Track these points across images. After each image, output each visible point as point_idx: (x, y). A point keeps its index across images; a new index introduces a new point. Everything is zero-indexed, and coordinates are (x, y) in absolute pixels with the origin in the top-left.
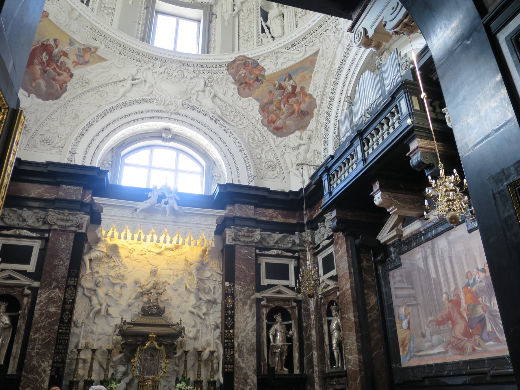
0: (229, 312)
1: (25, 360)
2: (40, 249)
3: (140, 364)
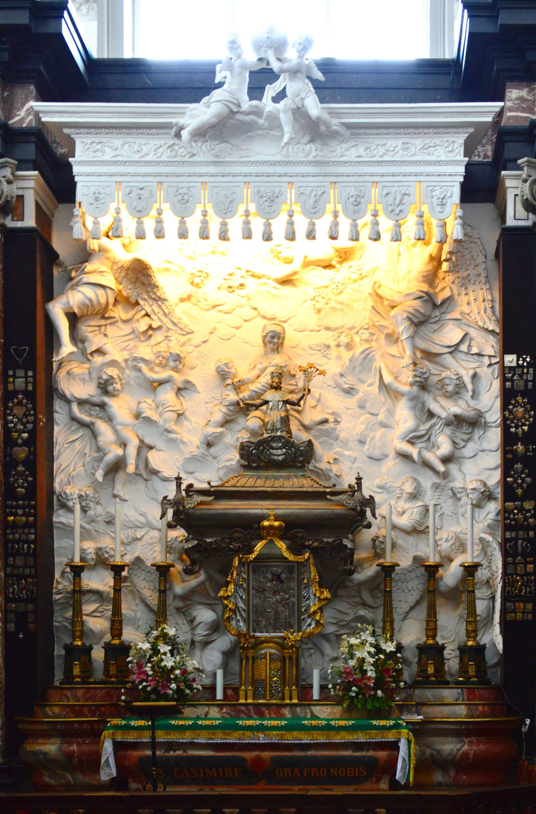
3: (247, 602)
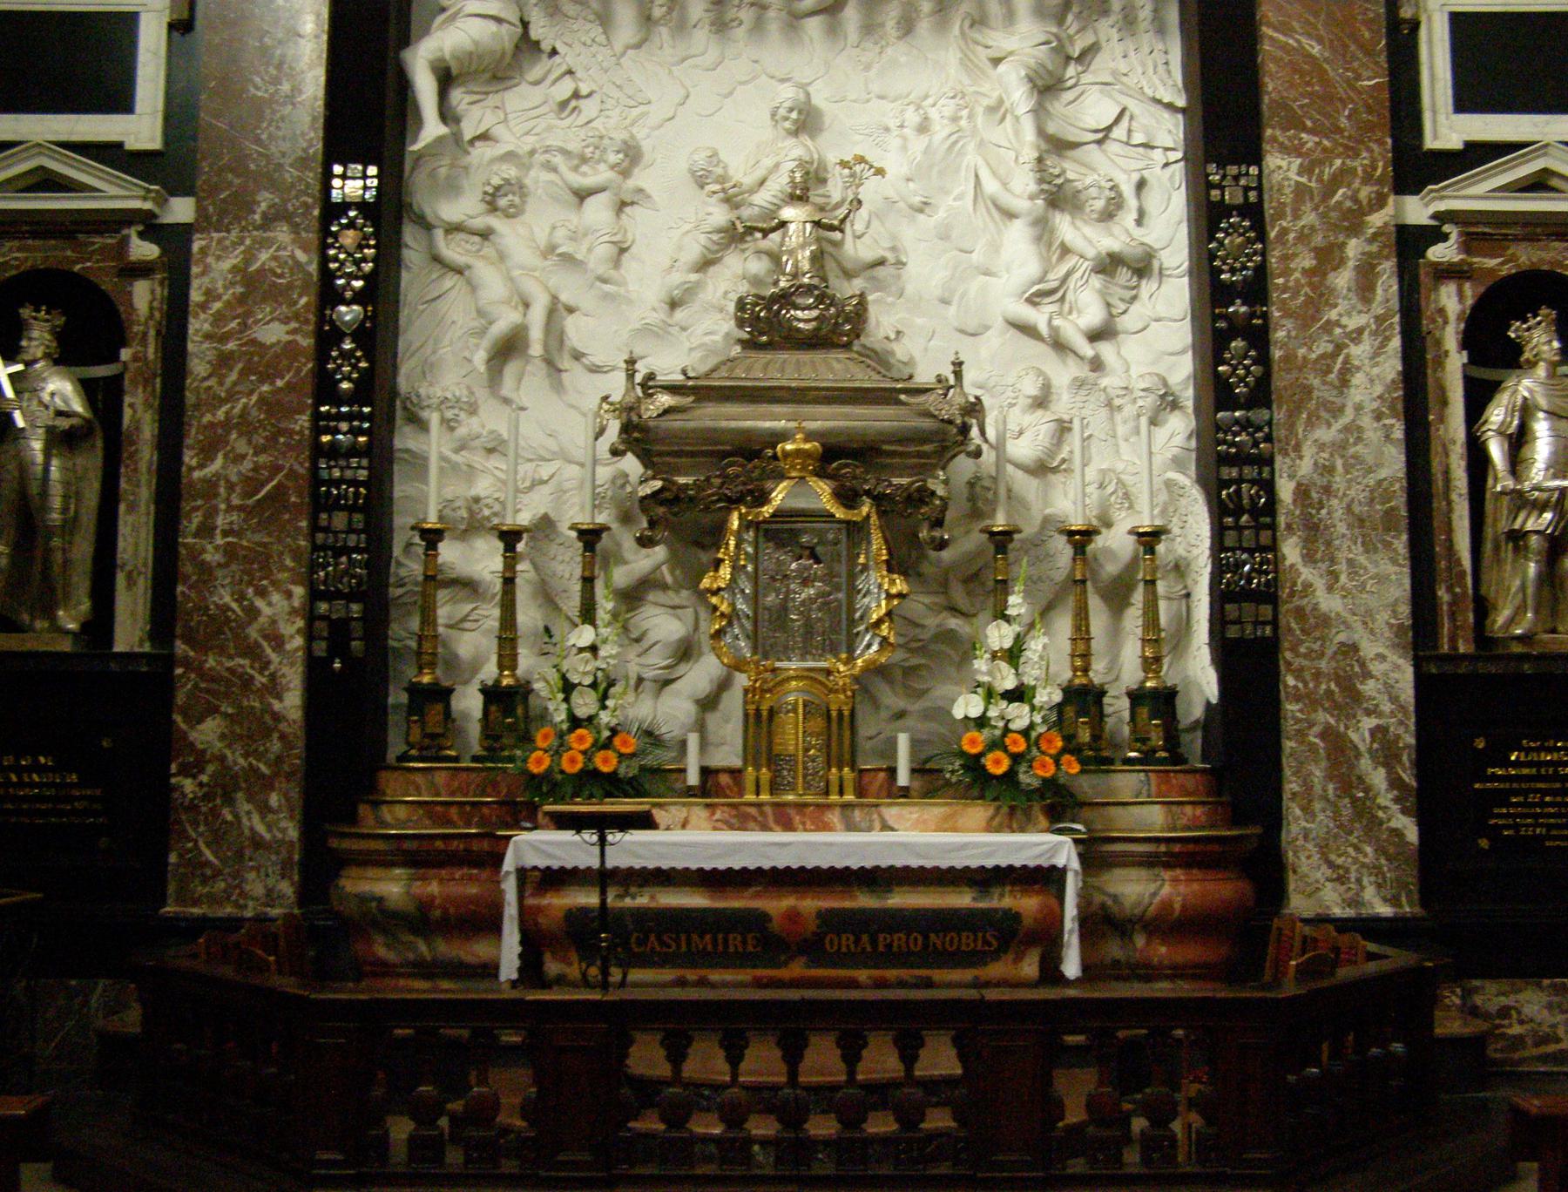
0: (1239, 308)
1: (180, 588)
2: (172, 27)
3: (755, 600)
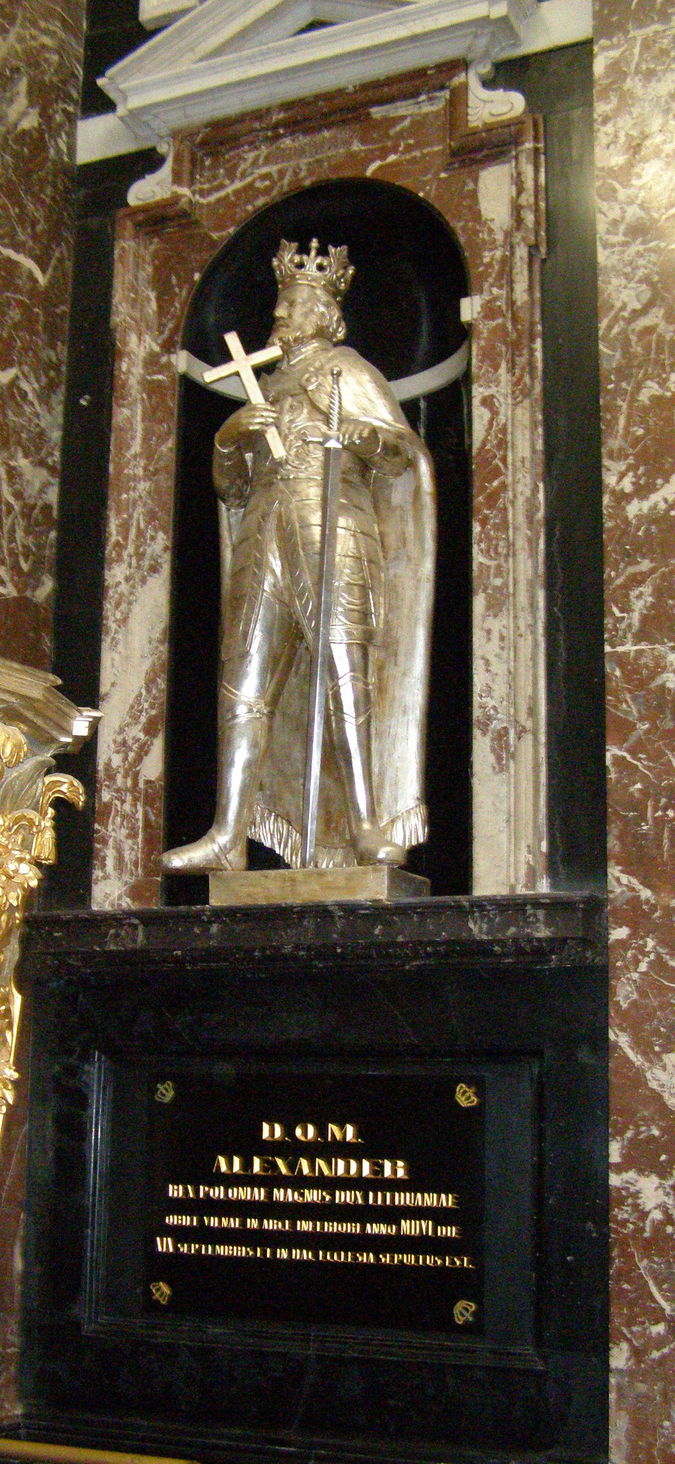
1: (612, 752)
